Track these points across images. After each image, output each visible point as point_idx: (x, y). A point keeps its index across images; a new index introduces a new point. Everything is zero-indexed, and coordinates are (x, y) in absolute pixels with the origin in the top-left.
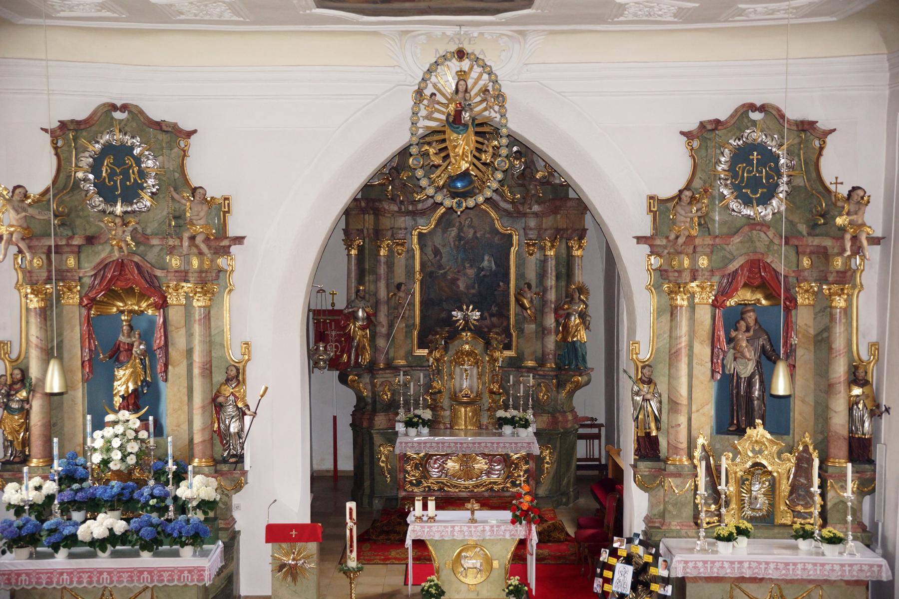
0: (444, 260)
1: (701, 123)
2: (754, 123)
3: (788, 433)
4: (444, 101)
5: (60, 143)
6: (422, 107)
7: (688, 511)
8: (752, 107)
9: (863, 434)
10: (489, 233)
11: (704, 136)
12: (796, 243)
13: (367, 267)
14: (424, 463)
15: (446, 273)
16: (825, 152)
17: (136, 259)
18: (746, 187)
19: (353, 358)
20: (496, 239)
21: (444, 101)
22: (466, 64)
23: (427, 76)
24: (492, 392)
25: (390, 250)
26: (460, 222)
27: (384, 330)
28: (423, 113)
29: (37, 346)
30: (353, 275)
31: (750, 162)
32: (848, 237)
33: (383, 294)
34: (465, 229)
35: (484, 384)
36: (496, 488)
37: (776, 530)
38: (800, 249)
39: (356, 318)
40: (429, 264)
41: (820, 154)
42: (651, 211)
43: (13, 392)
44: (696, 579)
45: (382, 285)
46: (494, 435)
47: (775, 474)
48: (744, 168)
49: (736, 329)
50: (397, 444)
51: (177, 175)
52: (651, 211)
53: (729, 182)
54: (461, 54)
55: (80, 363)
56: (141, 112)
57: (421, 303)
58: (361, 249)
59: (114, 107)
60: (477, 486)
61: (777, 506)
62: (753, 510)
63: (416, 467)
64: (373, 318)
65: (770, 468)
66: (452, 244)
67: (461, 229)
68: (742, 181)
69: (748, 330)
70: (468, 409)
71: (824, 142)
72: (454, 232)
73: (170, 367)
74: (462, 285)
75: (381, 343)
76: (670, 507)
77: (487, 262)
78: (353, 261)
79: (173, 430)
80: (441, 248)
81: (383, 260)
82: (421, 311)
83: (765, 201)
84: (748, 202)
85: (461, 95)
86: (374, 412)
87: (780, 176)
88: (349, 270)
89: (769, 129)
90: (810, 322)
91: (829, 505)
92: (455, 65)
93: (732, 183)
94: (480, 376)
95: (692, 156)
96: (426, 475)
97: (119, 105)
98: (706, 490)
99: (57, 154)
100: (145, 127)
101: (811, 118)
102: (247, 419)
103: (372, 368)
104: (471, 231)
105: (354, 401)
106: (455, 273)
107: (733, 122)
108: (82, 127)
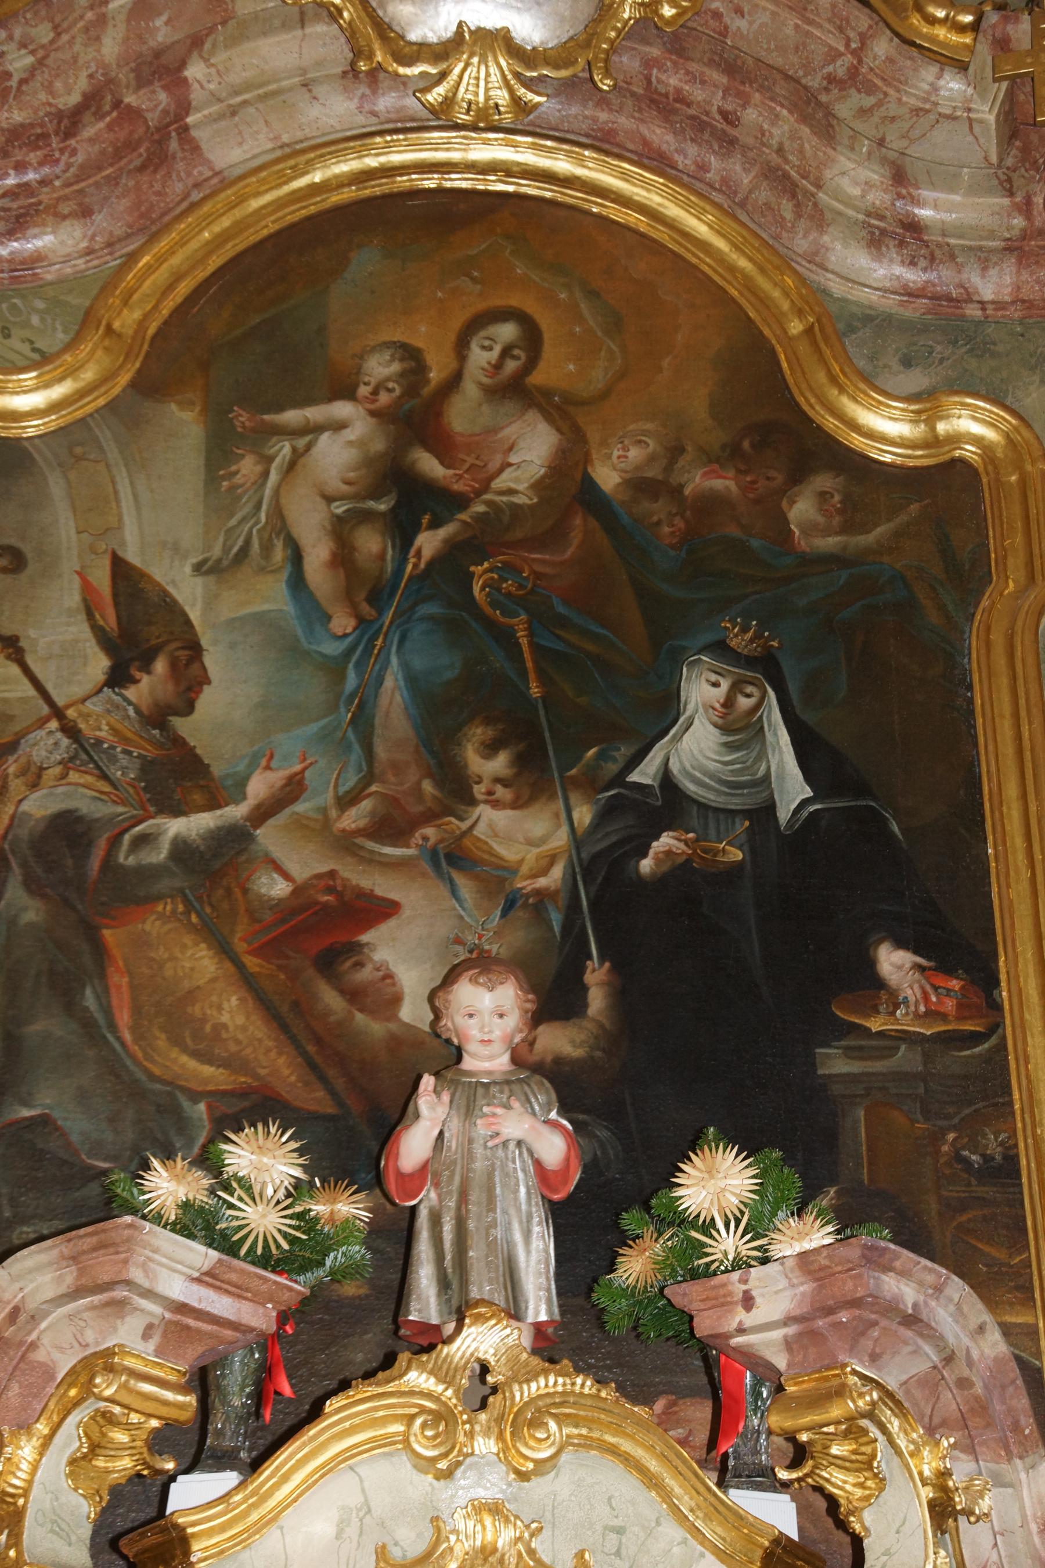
0: (224, 711)
10: (730, 455)
15: (234, 841)
20: (802, 510)
26: (413, 358)
34: (464, 414)
40: (46, 745)
66: (317, 554)
67: (416, 416)
72: (341, 443)
80: (189, 592)
106: (346, 844)
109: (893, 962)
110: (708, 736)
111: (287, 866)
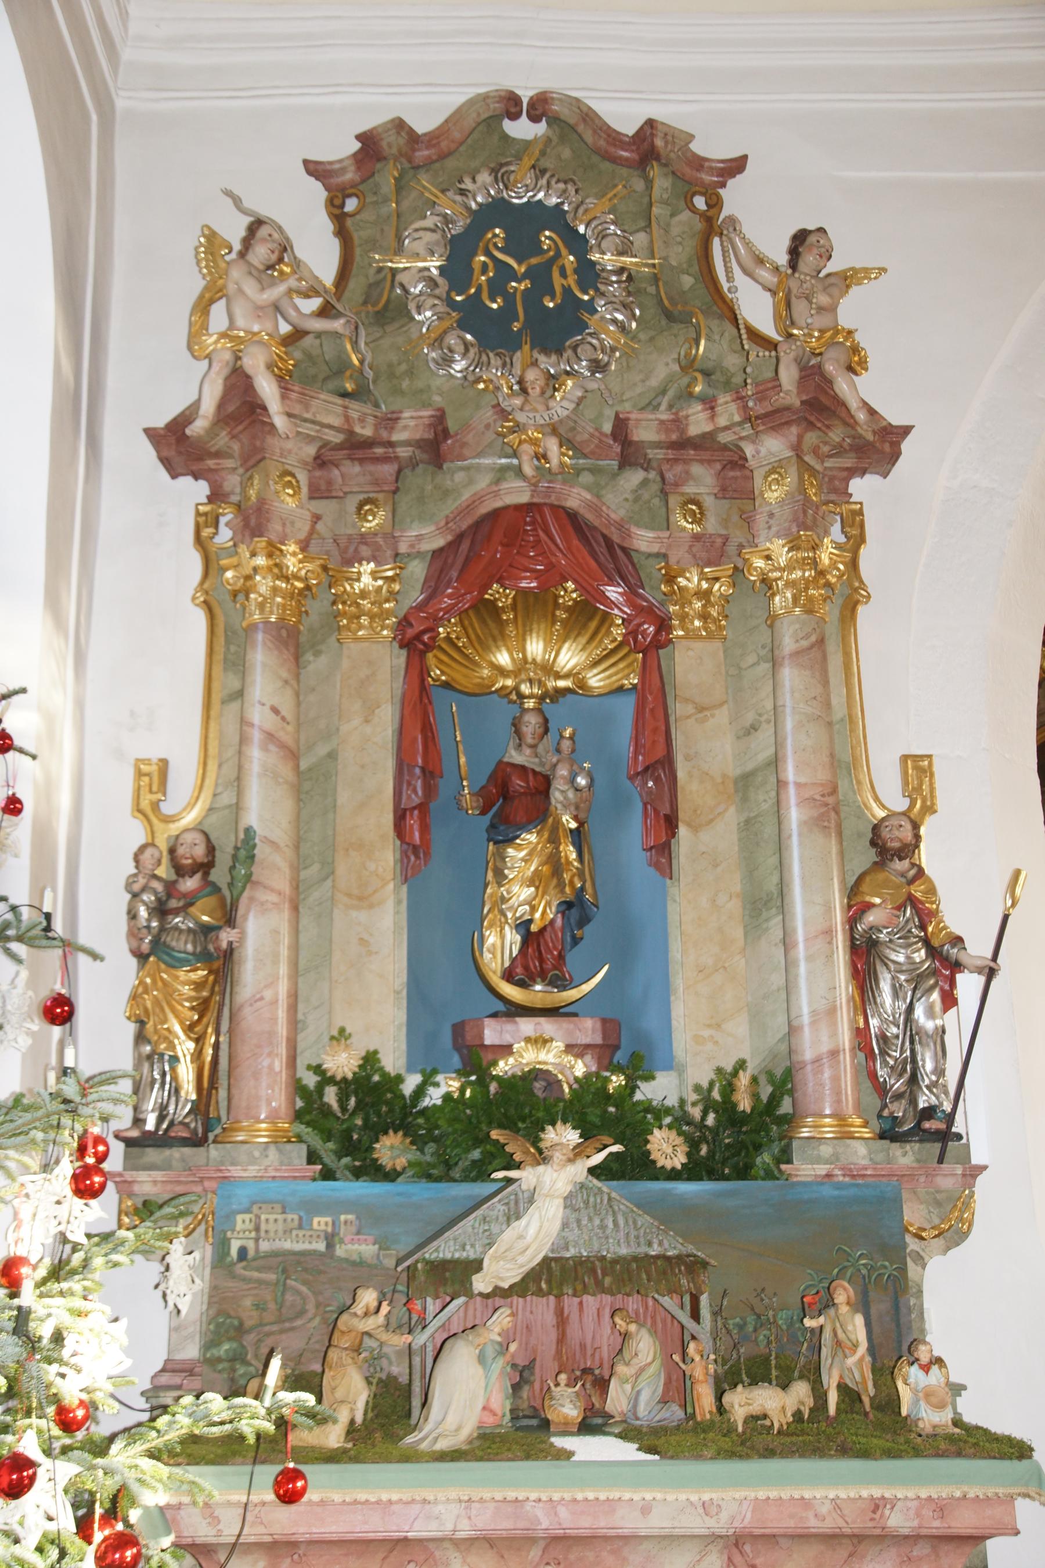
5: (351, 205)
17: (576, 498)
29: (270, 737)
43: (173, 903)
51: (687, 281)
55: (389, 819)
56: (589, 116)
59: (511, 105)
73: (682, 831)
79: (698, 1040)
97: (526, 96)
99: (342, 233)
100: (595, 159)
102: (968, 985)
108: (422, 154)
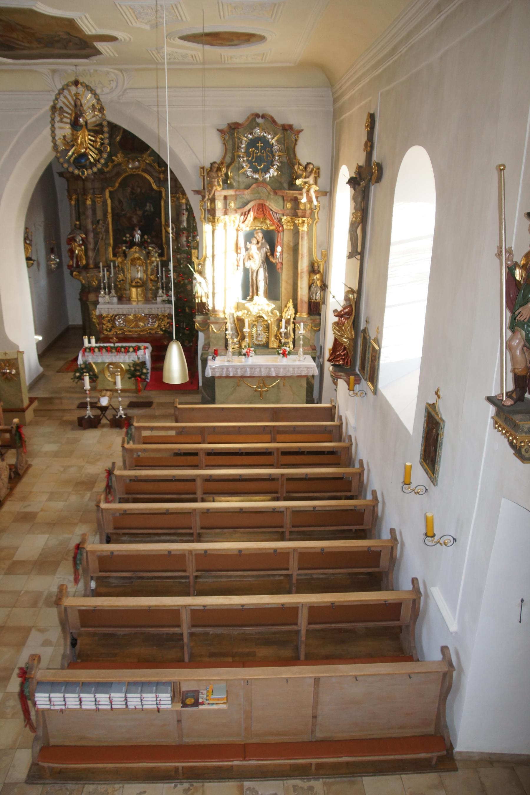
1: (228, 124)
2: (258, 125)
3: (278, 300)
4: (70, 112)
6: (56, 115)
7: (223, 342)
8: (257, 116)
9: (316, 300)
11: (231, 132)
12: (281, 194)
13: (81, 210)
14: (113, 320)
16: (298, 143)
18: (255, 162)
19: (75, 262)
21: (70, 112)
22: (81, 89)
23: (58, 96)
24: (151, 280)
25: (93, 202)
27: (91, 246)
28: (57, 119)
30: (74, 215)
31: (257, 148)
32: (304, 191)
33: (90, 227)
35: (147, 275)
36: (153, 332)
37: (270, 350)
38: (285, 198)
39: (76, 241)
41: (296, 144)
42: (201, 176)
44: (220, 377)
45: (89, 221)
46: (153, 303)
47: (269, 322)
48: (254, 151)
49: (250, 243)
50: (97, 310)
52: (201, 176)
53: (245, 159)
54: (76, 83)
57: (114, 231)
58: (77, 200)
60: (142, 331)
61: (270, 338)
62: (257, 340)
63: (109, 321)
64: (85, 240)
65: (266, 318)
67: (133, 188)
68: (252, 158)
69: (258, 243)
70: (139, 289)
71: (298, 137)
72: (129, 190)
74: (135, 220)
75: (91, 254)
76: (212, 340)
77: (149, 207)
78: (73, 208)
80: (122, 199)
81: (89, 207)
82: (114, 236)
83: (266, 170)
84: (256, 171)
85: (78, 108)
86: (89, 292)
87: (274, 156)
88: (71, 213)
89: (267, 128)
90: (291, 239)
91: (296, 337)
92: (73, 89)
93: (247, 160)
94: (145, 272)
95: (224, 144)
96: (114, 326)
98: (231, 331)
101: (291, 123)
103: (86, 268)
104: (139, 190)
105: (80, 287)
107: (247, 123)
109: (157, 219)
110: (149, 207)
111: (128, 215)
